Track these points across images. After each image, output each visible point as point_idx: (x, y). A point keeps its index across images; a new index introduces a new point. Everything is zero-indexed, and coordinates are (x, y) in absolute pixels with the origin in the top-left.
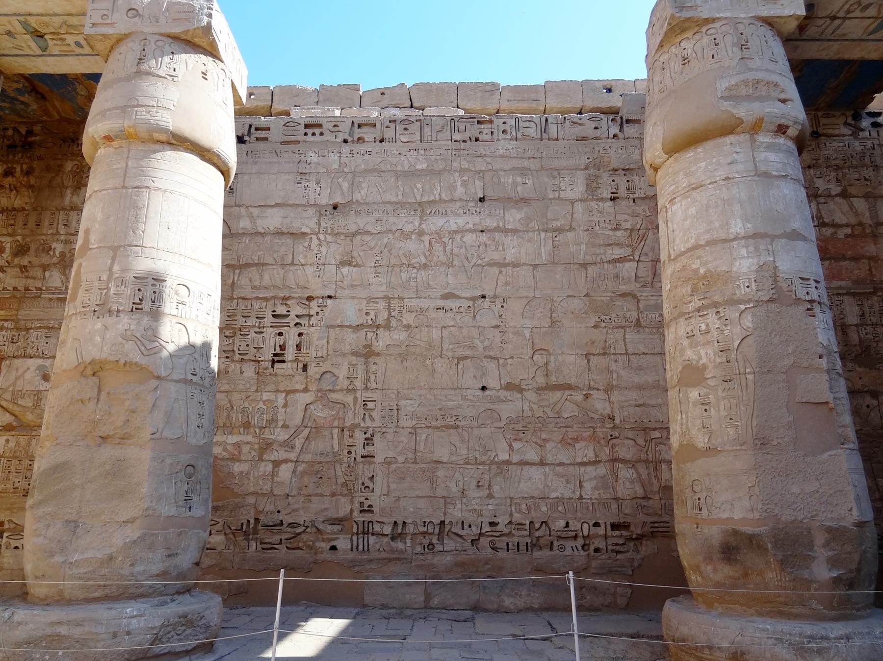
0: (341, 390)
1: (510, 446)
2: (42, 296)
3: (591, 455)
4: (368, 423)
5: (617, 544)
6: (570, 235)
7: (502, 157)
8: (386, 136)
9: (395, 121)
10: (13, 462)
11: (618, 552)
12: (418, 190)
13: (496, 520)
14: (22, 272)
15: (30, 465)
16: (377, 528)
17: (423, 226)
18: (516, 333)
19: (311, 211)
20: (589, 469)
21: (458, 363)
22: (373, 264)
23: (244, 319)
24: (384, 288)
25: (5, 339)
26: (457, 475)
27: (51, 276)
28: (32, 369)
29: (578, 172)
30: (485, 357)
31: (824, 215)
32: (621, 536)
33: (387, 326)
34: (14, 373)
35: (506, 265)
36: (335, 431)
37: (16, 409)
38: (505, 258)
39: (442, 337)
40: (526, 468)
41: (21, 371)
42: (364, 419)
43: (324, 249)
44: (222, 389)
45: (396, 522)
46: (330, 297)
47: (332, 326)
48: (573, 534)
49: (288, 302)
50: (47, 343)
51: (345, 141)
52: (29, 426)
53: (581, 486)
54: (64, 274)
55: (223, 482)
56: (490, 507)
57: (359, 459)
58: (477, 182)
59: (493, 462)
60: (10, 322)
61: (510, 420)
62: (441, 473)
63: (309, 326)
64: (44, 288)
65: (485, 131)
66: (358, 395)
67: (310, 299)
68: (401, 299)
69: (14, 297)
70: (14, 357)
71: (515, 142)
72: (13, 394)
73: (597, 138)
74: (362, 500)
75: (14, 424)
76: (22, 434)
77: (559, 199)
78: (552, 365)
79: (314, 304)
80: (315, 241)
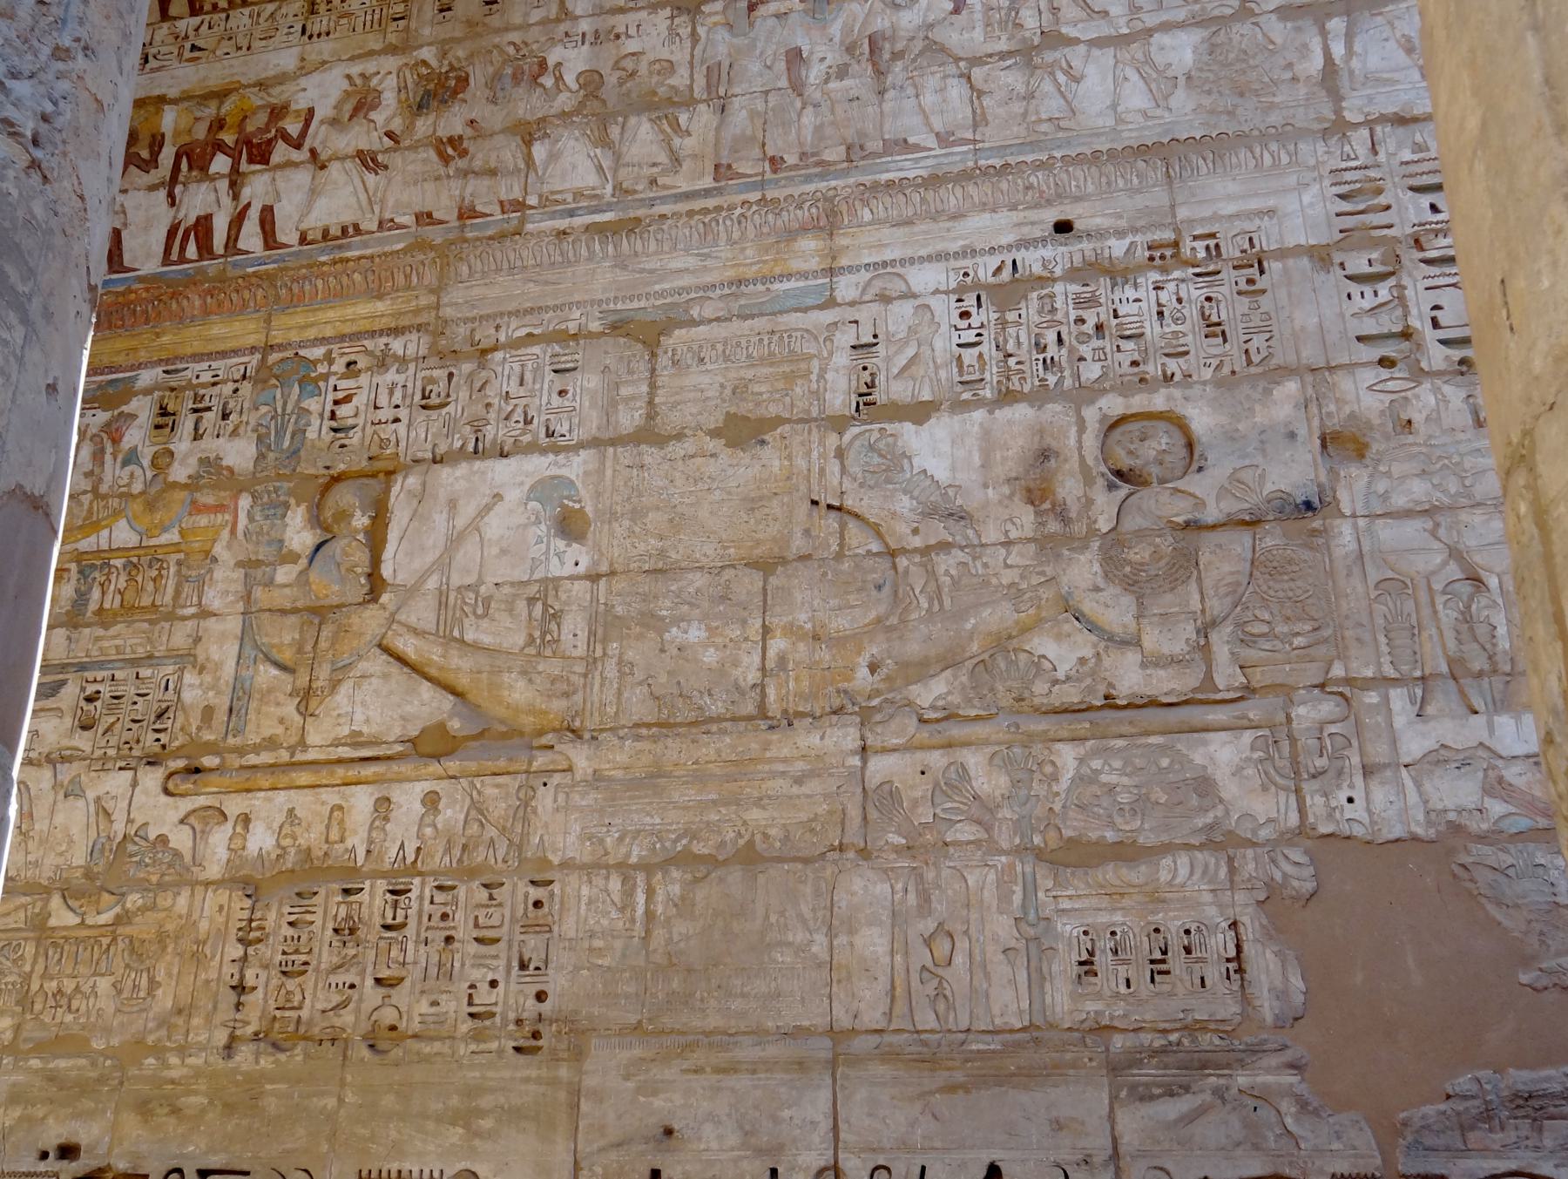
2: (529, 227)
10: (462, 892)
14: (446, 160)
15: (538, 904)
23: (1425, 200)
25: (397, 398)
27: (553, 157)
28: (513, 495)
34: (440, 519)
37: (460, 666)
41: (467, 511)
44: (1399, 501)
50: (562, 393)
52: (514, 733)
54: (604, 142)
55: (1527, 961)
60: (414, 336)
64: (532, 200)
69: (421, 245)
70: (435, 461)
72: (442, 603)
75: (455, 725)
76: (491, 765)
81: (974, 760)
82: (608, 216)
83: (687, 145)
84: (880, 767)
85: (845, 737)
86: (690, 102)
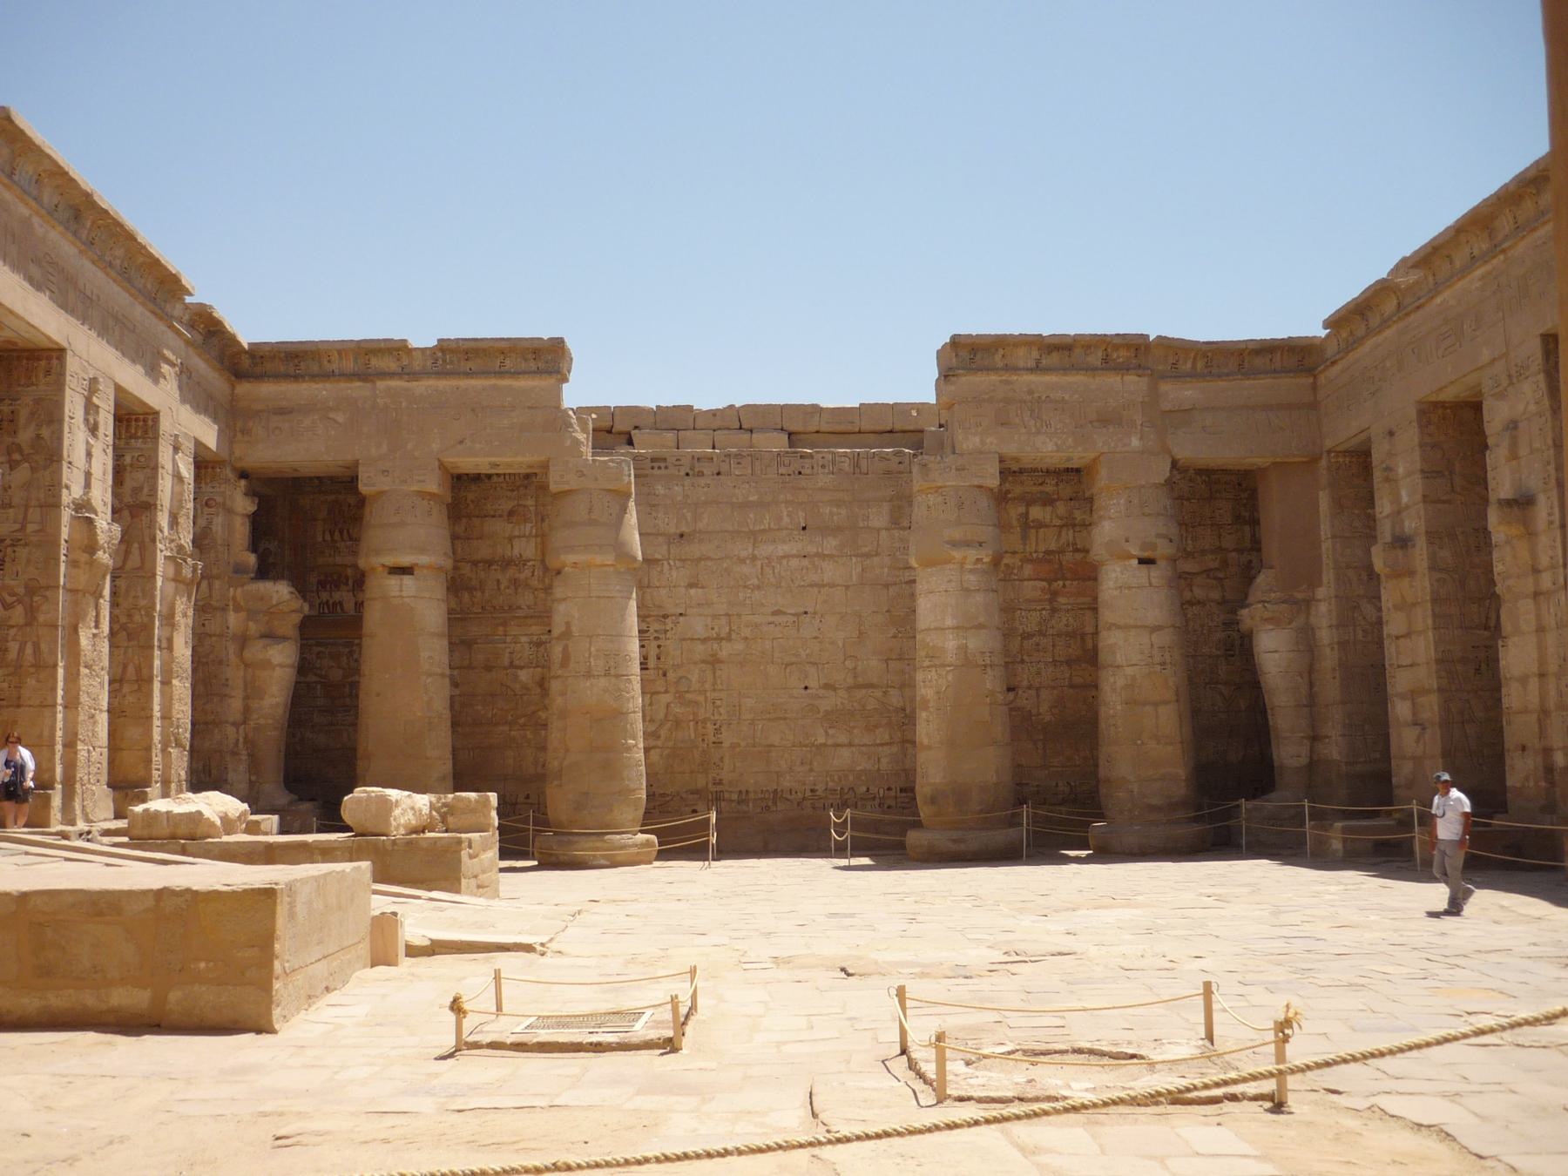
0: (695, 691)
1: (826, 732)
3: (887, 737)
4: (717, 717)
5: (903, 803)
6: (876, 560)
7: (821, 489)
8: (722, 470)
9: (730, 455)
11: (904, 808)
12: (751, 519)
13: (816, 788)
16: (727, 795)
17: (756, 552)
18: (832, 643)
19: (661, 539)
20: (885, 748)
21: (785, 669)
22: (715, 586)
24: (725, 606)
26: (786, 755)
29: (885, 504)
30: (808, 663)
31: (1078, 542)
32: (907, 797)
33: (729, 638)
35: (824, 586)
36: (692, 723)
38: (823, 581)
39: (773, 648)
40: (839, 748)
42: (713, 715)
43: (674, 574)
45: (740, 792)
46: (681, 614)
47: (684, 639)
48: (872, 796)
49: (648, 620)
51: (687, 474)
53: (879, 761)
54: (457, 596)
56: (811, 778)
57: (711, 745)
58: (800, 513)
59: (813, 745)
61: (827, 713)
62: (773, 754)
63: (666, 639)
65: (807, 466)
66: (708, 694)
67: (665, 616)
68: (739, 615)
71: (831, 476)
73: (900, 472)
74: (715, 775)
77: (868, 527)
78: (859, 668)
79: (668, 621)
80: (666, 566)
81: (528, 733)
82: (459, 616)
83: (476, 600)
84: (513, 733)
85: (506, 728)
86: (476, 589)
